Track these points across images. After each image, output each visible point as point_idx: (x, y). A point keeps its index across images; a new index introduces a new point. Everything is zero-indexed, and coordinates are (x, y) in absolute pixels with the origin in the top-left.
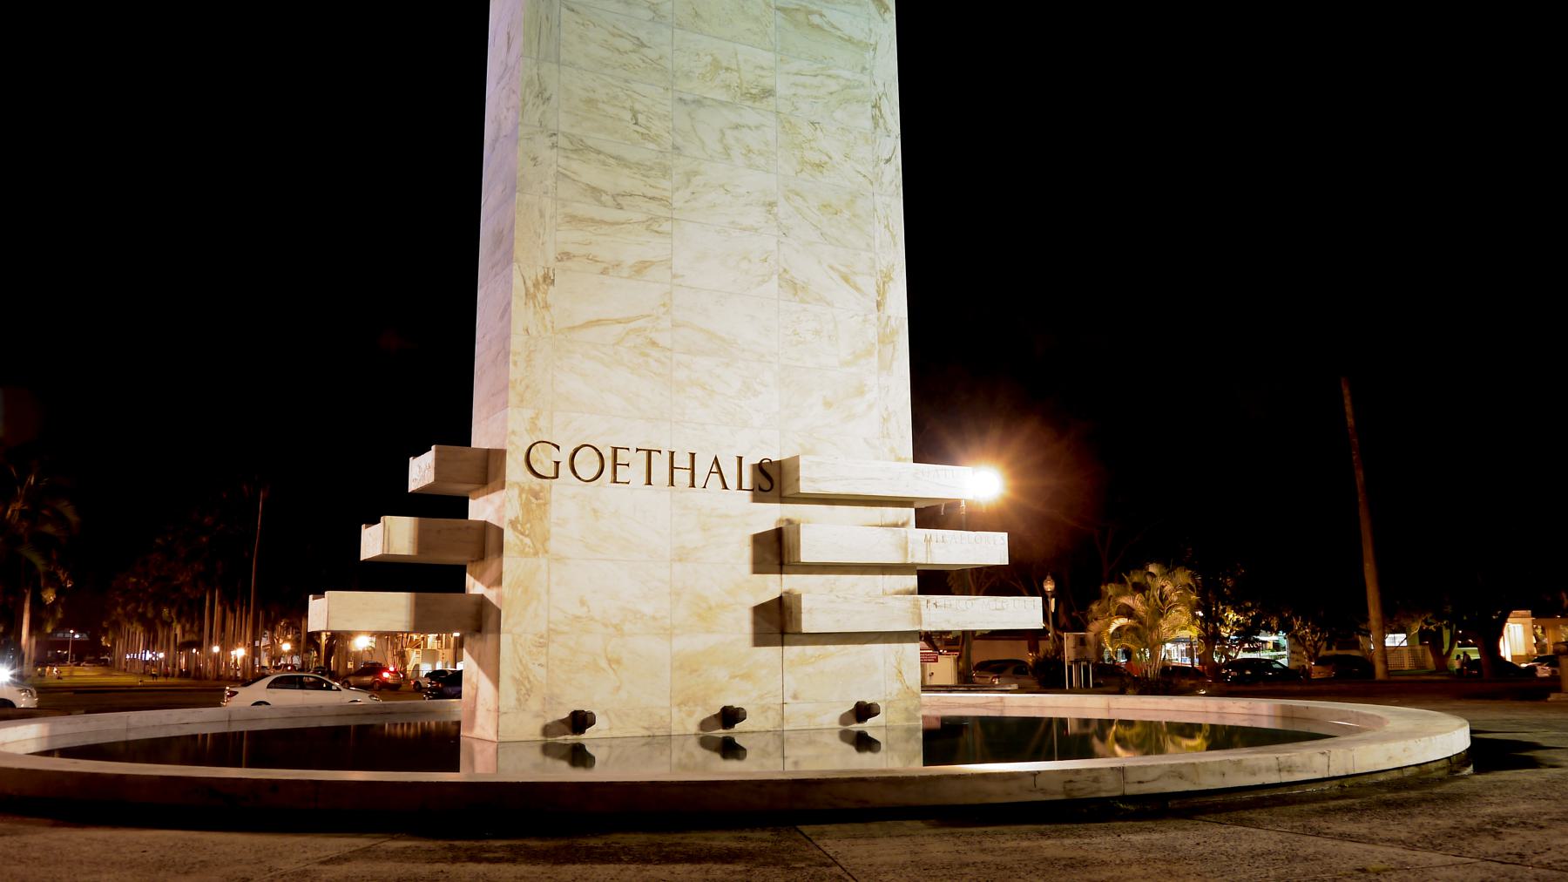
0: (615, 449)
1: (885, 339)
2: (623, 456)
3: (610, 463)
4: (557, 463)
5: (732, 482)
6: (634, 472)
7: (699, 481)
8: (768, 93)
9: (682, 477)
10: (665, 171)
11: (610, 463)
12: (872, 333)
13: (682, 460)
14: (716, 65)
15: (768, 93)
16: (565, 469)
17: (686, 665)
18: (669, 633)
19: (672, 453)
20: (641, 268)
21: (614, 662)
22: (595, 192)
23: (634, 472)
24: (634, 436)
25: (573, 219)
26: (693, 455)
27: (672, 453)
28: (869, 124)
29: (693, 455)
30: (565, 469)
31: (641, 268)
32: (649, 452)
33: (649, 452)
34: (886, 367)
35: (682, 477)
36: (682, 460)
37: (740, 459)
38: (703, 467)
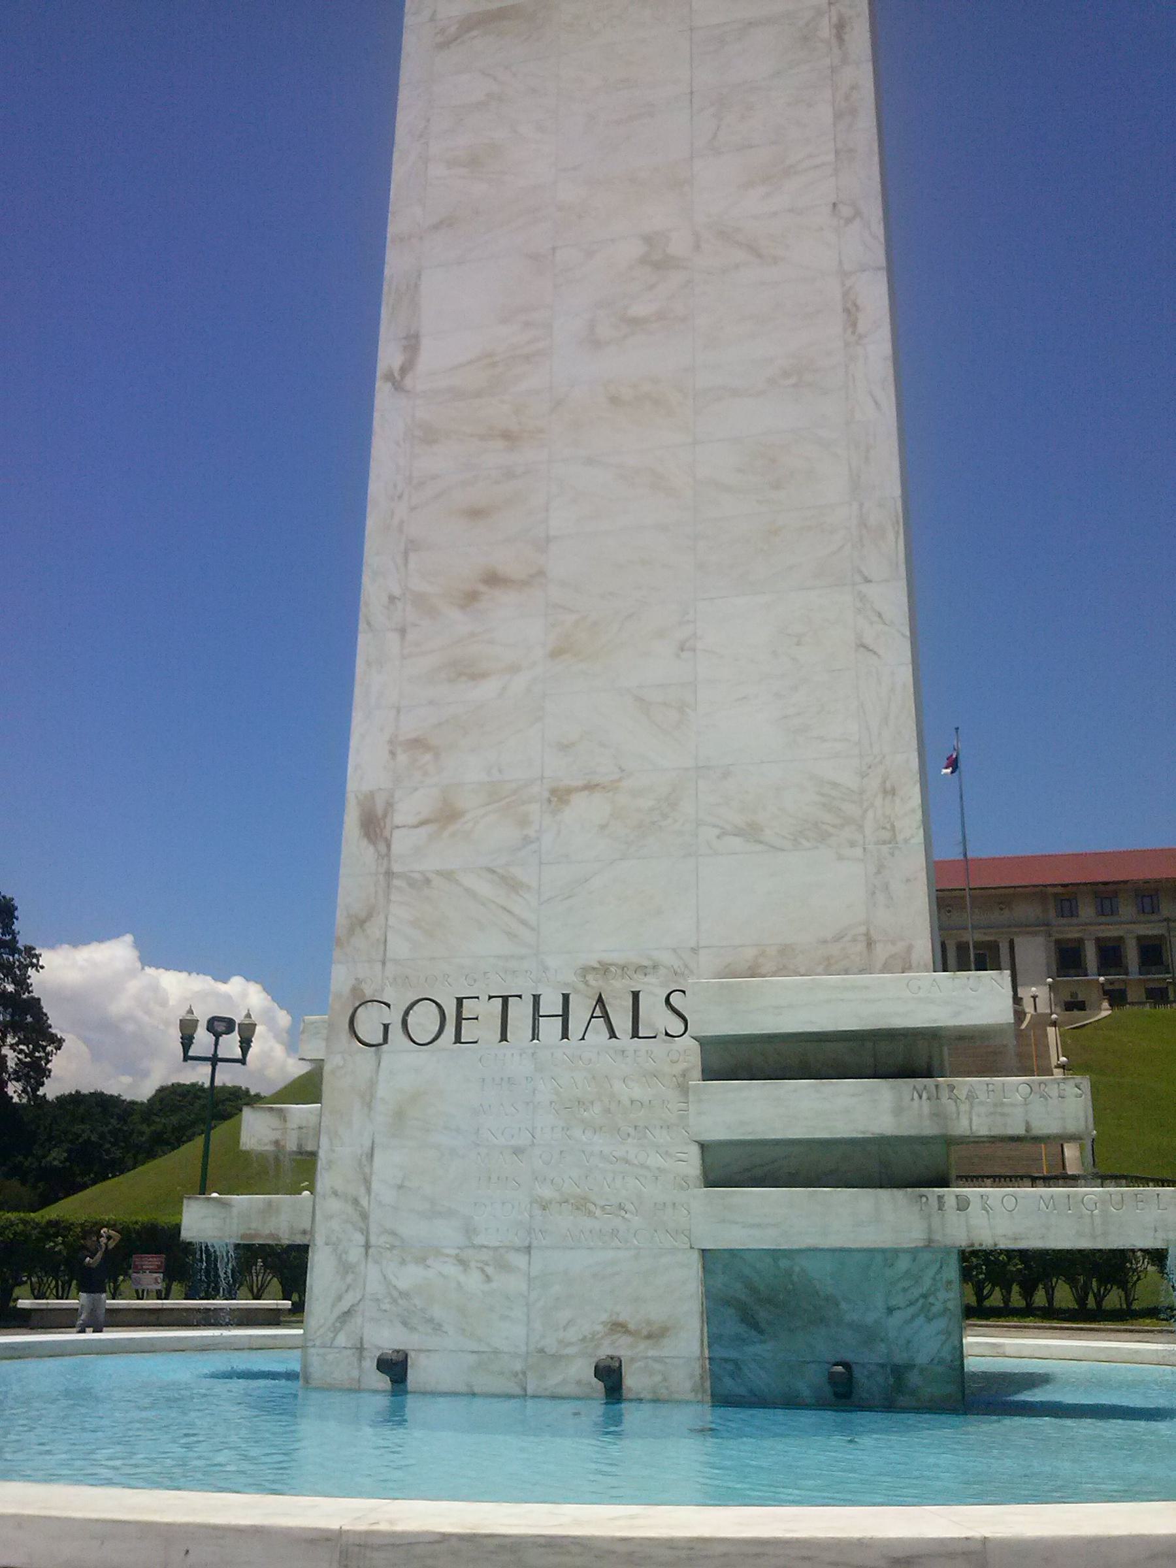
0: (460, 1001)
2: (469, 1008)
3: (455, 1020)
4: (386, 1027)
5: (622, 1023)
6: (483, 1029)
7: (575, 1027)
11: (455, 1020)
16: (396, 1032)
19: (536, 999)
23: (483, 1029)
26: (566, 998)
27: (536, 999)
29: (566, 998)
30: (396, 1032)
32: (505, 999)
33: (505, 999)
35: (550, 1028)
36: (551, 1004)
37: (636, 995)
38: (580, 1012)
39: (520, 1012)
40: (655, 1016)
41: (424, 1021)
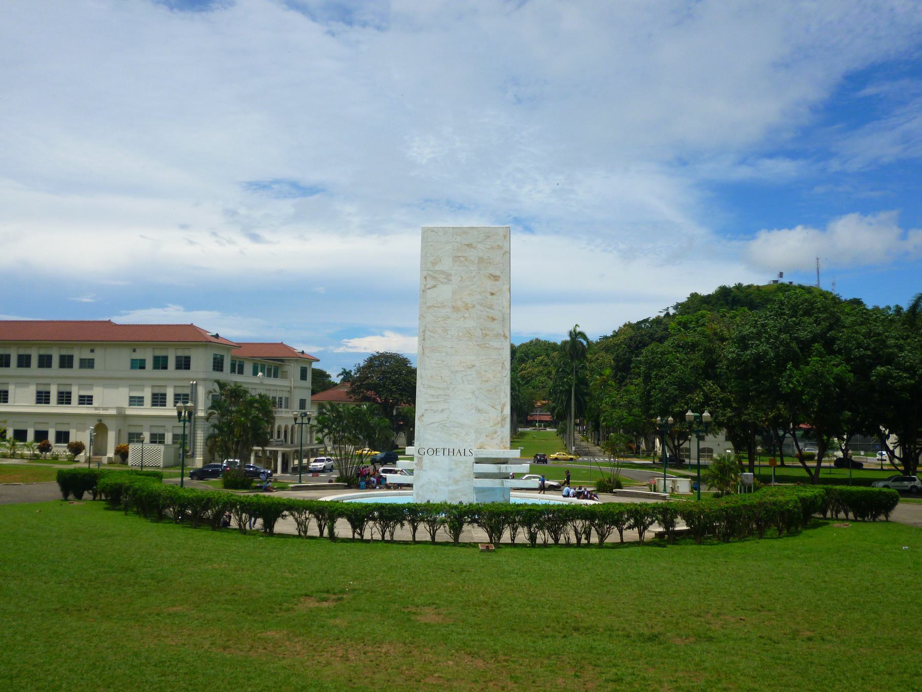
1: (503, 419)
3: (436, 451)
8: (474, 366)
9: (451, 454)
10: (448, 389)
11: (436, 451)
12: (499, 419)
13: (451, 450)
14: (461, 362)
15: (474, 366)
17: (452, 492)
18: (448, 486)
20: (442, 411)
21: (436, 491)
22: (433, 395)
23: (441, 453)
24: (440, 446)
25: (429, 402)
28: (500, 368)
31: (442, 411)
34: (503, 426)
35: (451, 454)
36: (451, 450)
39: (446, 452)
40: (467, 453)
41: (431, 452)
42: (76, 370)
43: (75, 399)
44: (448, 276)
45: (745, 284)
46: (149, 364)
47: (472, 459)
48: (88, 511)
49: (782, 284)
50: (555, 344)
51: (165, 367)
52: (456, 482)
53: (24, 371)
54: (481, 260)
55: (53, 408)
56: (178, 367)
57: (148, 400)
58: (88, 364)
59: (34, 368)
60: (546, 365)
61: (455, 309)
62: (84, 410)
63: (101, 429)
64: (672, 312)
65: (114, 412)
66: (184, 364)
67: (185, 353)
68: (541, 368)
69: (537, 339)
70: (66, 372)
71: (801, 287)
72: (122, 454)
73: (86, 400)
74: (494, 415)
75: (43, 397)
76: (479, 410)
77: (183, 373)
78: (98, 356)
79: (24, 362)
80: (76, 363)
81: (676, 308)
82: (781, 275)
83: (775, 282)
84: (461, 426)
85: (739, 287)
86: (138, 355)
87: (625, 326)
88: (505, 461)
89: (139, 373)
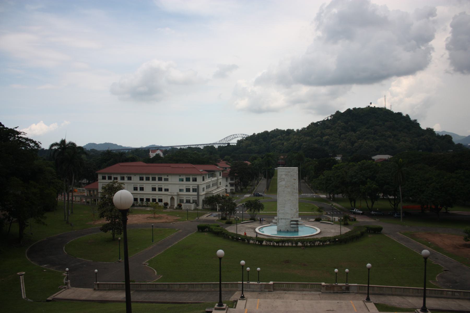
3: (282, 219)
11: (282, 219)
42: (163, 182)
43: (163, 190)
44: (284, 179)
45: (357, 107)
46: (185, 180)
47: (290, 220)
48: (206, 235)
49: (371, 107)
50: (284, 130)
51: (189, 181)
52: (287, 225)
53: (148, 182)
54: (291, 175)
55: (157, 192)
56: (193, 181)
57: (185, 190)
58: (166, 180)
59: (151, 181)
60: (281, 140)
61: (286, 187)
62: (166, 193)
63: (172, 199)
64: (329, 118)
65: (176, 194)
66: (195, 180)
67: (195, 177)
68: (279, 141)
69: (277, 129)
70: (160, 182)
71: (378, 108)
72: (180, 206)
73: (167, 190)
74: (295, 210)
75: (154, 189)
76: (292, 210)
77: (195, 183)
78: (169, 178)
79: (148, 179)
80: (163, 179)
81: (331, 117)
82: (371, 103)
83: (369, 106)
84: (288, 213)
85: (354, 109)
86: (181, 177)
87: (311, 124)
88: (298, 221)
89: (182, 182)
